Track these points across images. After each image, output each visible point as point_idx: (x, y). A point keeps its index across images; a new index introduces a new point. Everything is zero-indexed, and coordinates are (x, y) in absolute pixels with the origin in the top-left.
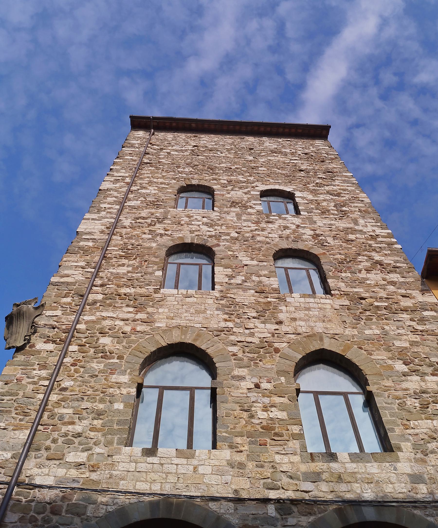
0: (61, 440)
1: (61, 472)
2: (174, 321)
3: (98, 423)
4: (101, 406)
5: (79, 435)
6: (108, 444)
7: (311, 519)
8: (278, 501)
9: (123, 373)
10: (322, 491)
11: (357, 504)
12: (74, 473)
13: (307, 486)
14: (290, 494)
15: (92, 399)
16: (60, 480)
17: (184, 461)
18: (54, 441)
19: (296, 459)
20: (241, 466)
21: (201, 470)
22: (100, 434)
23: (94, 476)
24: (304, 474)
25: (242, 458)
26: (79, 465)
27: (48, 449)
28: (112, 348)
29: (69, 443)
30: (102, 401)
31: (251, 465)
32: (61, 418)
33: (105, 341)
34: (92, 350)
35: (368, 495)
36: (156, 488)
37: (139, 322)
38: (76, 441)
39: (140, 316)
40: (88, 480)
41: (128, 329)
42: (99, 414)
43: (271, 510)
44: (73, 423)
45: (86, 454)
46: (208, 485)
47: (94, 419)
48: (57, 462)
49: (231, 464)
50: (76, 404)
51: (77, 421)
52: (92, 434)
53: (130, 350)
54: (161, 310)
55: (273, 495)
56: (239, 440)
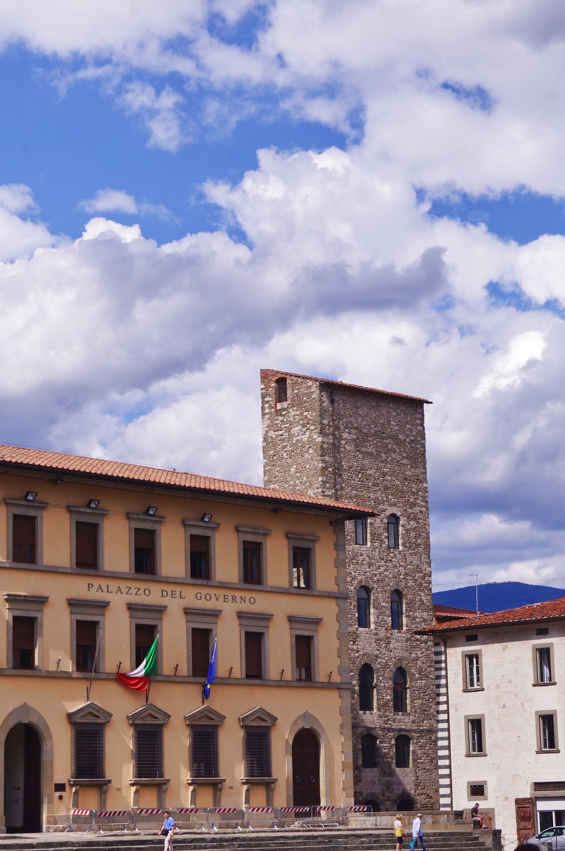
10: (395, 726)
11: (401, 730)
35: (403, 727)
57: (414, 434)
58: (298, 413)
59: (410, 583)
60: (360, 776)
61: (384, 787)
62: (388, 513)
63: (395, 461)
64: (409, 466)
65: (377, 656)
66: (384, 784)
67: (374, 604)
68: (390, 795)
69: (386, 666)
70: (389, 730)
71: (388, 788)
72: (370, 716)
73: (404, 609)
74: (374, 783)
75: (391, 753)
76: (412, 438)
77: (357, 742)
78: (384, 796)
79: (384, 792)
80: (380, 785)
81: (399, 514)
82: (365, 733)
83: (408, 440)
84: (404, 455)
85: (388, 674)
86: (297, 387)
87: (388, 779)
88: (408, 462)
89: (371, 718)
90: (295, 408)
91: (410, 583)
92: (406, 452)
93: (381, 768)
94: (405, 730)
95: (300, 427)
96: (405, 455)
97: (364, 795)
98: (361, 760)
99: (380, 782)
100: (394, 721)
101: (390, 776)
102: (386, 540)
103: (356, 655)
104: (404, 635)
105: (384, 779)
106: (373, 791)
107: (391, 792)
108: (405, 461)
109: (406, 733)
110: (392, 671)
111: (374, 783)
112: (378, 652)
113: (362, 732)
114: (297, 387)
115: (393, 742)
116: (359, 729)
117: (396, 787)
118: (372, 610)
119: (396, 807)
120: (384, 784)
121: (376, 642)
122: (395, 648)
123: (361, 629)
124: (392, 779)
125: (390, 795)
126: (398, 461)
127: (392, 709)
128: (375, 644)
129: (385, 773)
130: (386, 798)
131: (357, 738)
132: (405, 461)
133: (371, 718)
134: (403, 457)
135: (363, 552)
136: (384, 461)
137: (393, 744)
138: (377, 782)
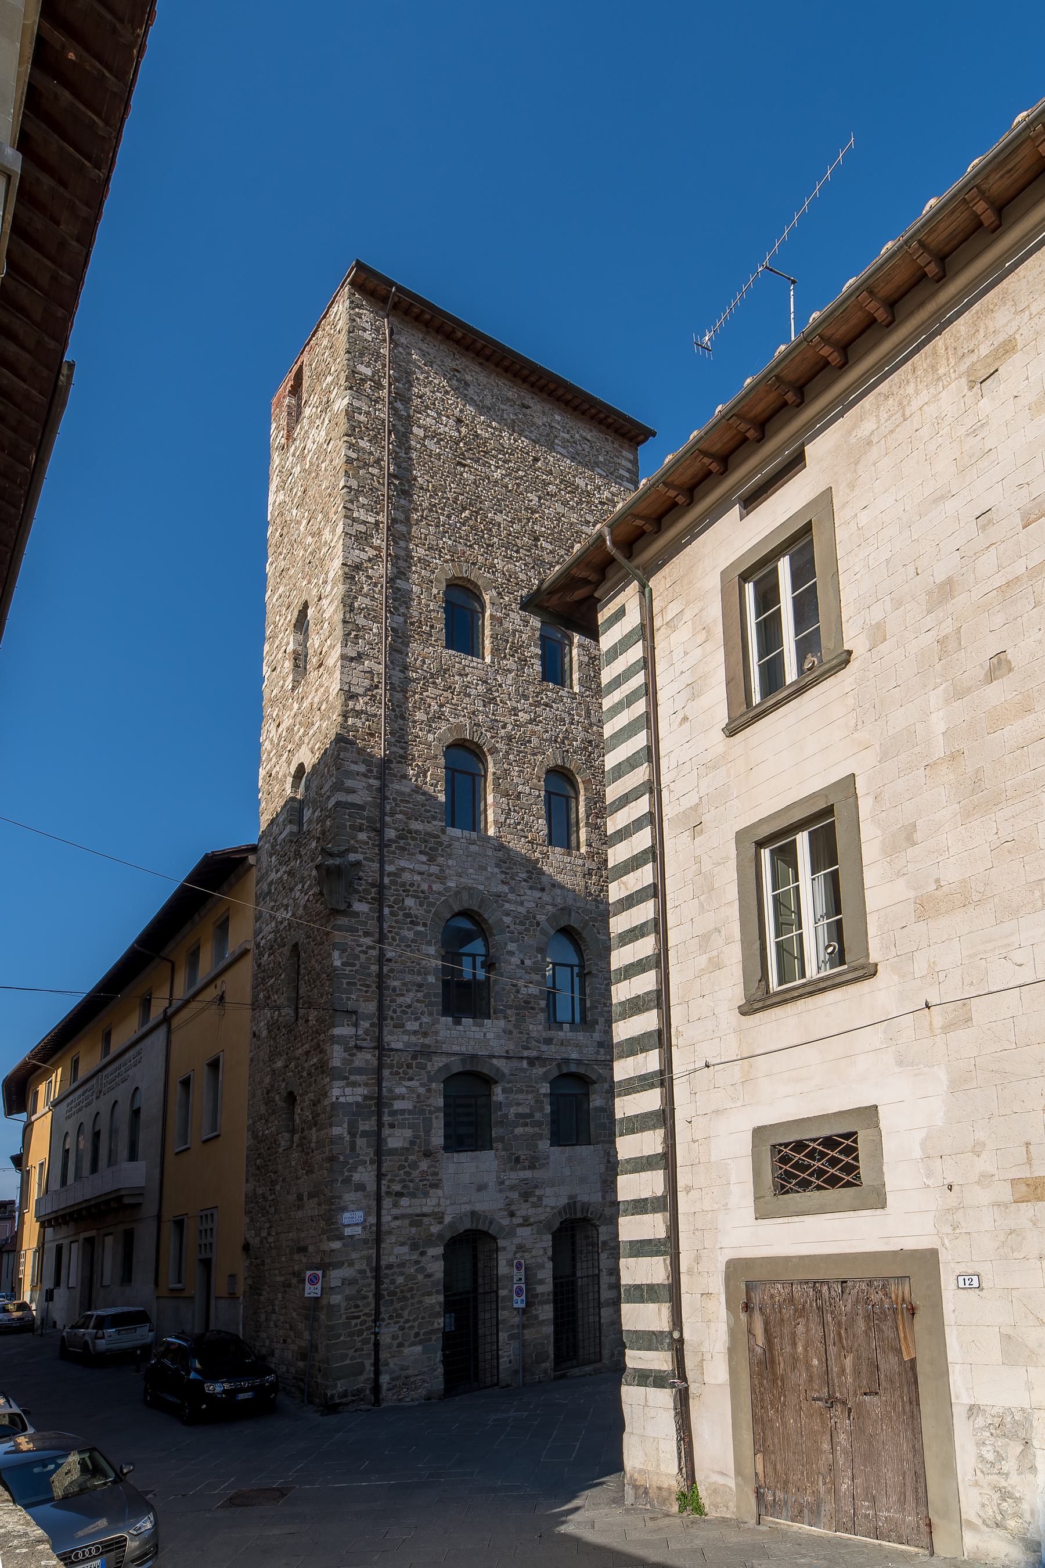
0: (399, 1010)
1: (406, 1038)
2: (462, 880)
3: (420, 995)
4: (419, 978)
5: (409, 1006)
6: (431, 1014)
7: (545, 1069)
8: (527, 1058)
9: (429, 943)
11: (567, 1061)
12: (413, 1039)
13: (544, 1048)
14: (535, 1054)
15: (412, 972)
16: (407, 1044)
17: (478, 1029)
18: (395, 1011)
19: (540, 1028)
20: (510, 1032)
21: (488, 1036)
23: (427, 1041)
24: (544, 1039)
25: (510, 1027)
26: (415, 1033)
27: (392, 1018)
28: (416, 912)
29: (404, 1012)
30: (419, 973)
31: (515, 1032)
32: (394, 990)
33: (409, 902)
34: (401, 913)
35: (574, 1056)
36: (464, 1049)
37: (433, 878)
38: (409, 1011)
39: (434, 869)
40: (423, 1045)
41: (425, 886)
42: (420, 986)
43: (525, 1064)
44: (403, 995)
45: (417, 1024)
46: (492, 1047)
47: (417, 991)
49: (504, 1031)
52: (419, 1005)
53: (431, 915)
54: (450, 862)
55: (526, 1053)
56: (509, 1012)
60: (436, 1174)
61: (515, 1195)
66: (512, 1188)
67: (497, 785)
68: (531, 1211)
69: (528, 920)
70: (532, 1062)
71: (526, 1196)
72: (474, 1029)
73: (582, 810)
74: (481, 1188)
75: (538, 1116)
77: (429, 1090)
78: (512, 1214)
79: (513, 1208)
80: (501, 1191)
82: (457, 1068)
87: (527, 1174)
89: (479, 1036)
93: (505, 1149)
94: (579, 1062)
97: (448, 1219)
98: (441, 1132)
99: (503, 1183)
100: (548, 1041)
101: (532, 1167)
103: (436, 887)
104: (580, 862)
105: (514, 1175)
106: (478, 1207)
107: (535, 1205)
109: (582, 1070)
110: (543, 932)
111: (481, 1188)
112: (506, 889)
113: (447, 1066)
115: (545, 1088)
116: (435, 1059)
117: (549, 1191)
118: (490, 799)
119: (550, 1237)
120: (512, 1188)
121: (497, 866)
123: (449, 829)
124: (538, 1174)
125: (531, 1211)
127: (542, 1016)
128: (496, 870)
129: (517, 1160)
130: (520, 1221)
131: (431, 1079)
137: (545, 1095)
138: (492, 1185)
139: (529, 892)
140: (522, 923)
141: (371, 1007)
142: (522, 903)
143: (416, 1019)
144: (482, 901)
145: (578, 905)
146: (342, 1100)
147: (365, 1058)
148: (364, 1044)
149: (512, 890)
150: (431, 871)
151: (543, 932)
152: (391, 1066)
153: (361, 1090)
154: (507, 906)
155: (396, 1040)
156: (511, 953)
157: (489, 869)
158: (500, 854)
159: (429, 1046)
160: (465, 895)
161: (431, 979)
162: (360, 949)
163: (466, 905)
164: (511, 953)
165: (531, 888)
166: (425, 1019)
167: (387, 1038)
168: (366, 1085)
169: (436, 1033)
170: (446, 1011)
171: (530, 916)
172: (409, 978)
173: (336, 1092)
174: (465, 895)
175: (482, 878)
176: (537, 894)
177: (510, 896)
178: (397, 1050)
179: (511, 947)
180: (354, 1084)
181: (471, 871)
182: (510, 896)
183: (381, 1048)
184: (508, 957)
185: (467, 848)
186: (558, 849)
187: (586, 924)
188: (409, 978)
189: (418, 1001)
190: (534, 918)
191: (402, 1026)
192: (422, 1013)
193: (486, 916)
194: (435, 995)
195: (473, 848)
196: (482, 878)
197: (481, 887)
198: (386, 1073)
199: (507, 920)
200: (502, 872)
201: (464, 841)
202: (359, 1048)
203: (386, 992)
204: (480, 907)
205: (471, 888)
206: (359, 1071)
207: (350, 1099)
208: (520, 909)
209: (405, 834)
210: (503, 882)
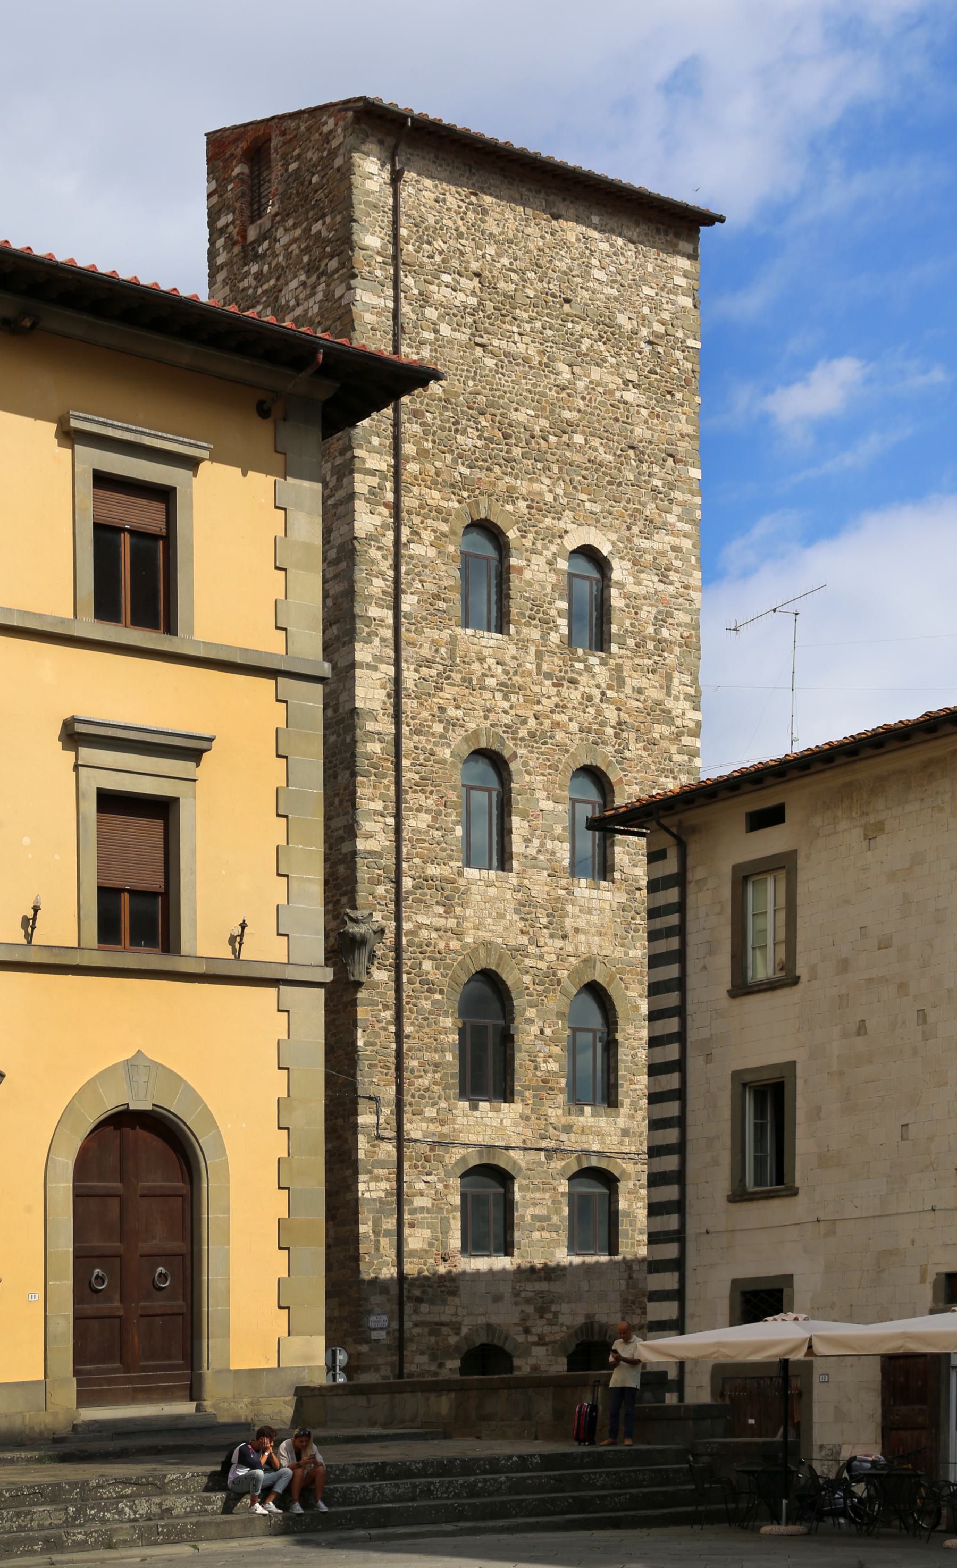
2: (480, 933)
3: (438, 1075)
6: (447, 1099)
12: (432, 1127)
18: (413, 1096)
22: (440, 1088)
26: (432, 1120)
27: (411, 1105)
29: (422, 1097)
30: (436, 1051)
38: (427, 1095)
42: (437, 1065)
44: (421, 1077)
47: (435, 1072)
48: (419, 1117)
50: (419, 1054)
51: (423, 1073)
52: (436, 1087)
57: (666, 316)
58: (298, 232)
59: (635, 750)
62: (571, 543)
63: (601, 390)
64: (644, 412)
65: (520, 951)
69: (549, 978)
76: (660, 329)
81: (605, 549)
83: (644, 332)
84: (628, 376)
85: (555, 1003)
86: (296, 153)
88: (643, 400)
90: (290, 222)
91: (635, 750)
92: (636, 368)
95: (303, 278)
96: (633, 376)
102: (563, 623)
108: (630, 396)
112: (525, 940)
114: (296, 153)
116: (453, 1150)
121: (516, 911)
122: (577, 930)
126: (612, 392)
128: (516, 917)
132: (630, 396)
133: (496, 1123)
134: (626, 382)
135: (486, 652)
136: (563, 389)
139: (550, 941)
140: (541, 983)
141: (391, 1091)
142: (541, 958)
143: (434, 1105)
144: (501, 958)
145: (604, 953)
146: (367, 1195)
147: (388, 1149)
148: (387, 1134)
149: (534, 942)
150: (448, 926)
151: (564, 993)
152: (410, 1159)
153: (385, 1185)
154: (528, 962)
155: (414, 1129)
156: (530, 1021)
157: (508, 917)
158: (519, 895)
159: (445, 1135)
160: (482, 952)
161: (449, 1057)
162: (380, 1025)
163: (484, 965)
164: (530, 1021)
165: (552, 936)
166: (443, 1105)
167: (407, 1126)
168: (388, 1180)
169: (454, 1121)
170: (463, 1095)
171: (552, 971)
172: (427, 1056)
173: (361, 1187)
174: (482, 952)
175: (500, 929)
176: (559, 943)
177: (532, 949)
178: (415, 1141)
179: (531, 1013)
180: (377, 1179)
181: (489, 921)
182: (532, 949)
183: (400, 1140)
184: (527, 1027)
185: (485, 891)
186: (583, 882)
187: (612, 977)
188: (427, 1056)
189: (435, 1083)
190: (555, 975)
191: (420, 1113)
192: (439, 1098)
193: (504, 977)
194: (452, 1076)
195: (492, 891)
196: (500, 929)
197: (500, 941)
198: (406, 1165)
199: (527, 979)
200: (522, 919)
201: (482, 883)
202: (380, 1138)
203: (405, 1075)
204: (498, 965)
205: (490, 943)
206: (382, 1164)
207: (375, 1195)
208: (542, 965)
209: (424, 881)
210: (522, 932)
